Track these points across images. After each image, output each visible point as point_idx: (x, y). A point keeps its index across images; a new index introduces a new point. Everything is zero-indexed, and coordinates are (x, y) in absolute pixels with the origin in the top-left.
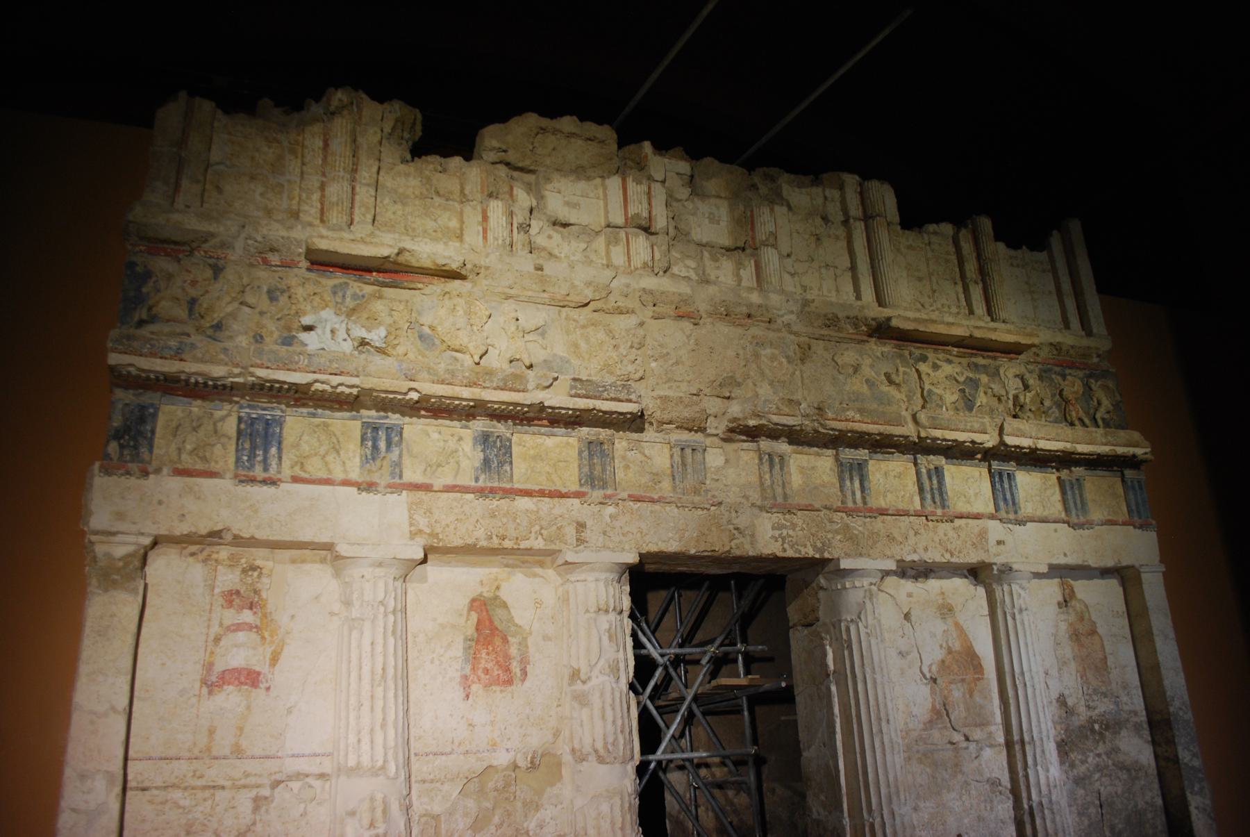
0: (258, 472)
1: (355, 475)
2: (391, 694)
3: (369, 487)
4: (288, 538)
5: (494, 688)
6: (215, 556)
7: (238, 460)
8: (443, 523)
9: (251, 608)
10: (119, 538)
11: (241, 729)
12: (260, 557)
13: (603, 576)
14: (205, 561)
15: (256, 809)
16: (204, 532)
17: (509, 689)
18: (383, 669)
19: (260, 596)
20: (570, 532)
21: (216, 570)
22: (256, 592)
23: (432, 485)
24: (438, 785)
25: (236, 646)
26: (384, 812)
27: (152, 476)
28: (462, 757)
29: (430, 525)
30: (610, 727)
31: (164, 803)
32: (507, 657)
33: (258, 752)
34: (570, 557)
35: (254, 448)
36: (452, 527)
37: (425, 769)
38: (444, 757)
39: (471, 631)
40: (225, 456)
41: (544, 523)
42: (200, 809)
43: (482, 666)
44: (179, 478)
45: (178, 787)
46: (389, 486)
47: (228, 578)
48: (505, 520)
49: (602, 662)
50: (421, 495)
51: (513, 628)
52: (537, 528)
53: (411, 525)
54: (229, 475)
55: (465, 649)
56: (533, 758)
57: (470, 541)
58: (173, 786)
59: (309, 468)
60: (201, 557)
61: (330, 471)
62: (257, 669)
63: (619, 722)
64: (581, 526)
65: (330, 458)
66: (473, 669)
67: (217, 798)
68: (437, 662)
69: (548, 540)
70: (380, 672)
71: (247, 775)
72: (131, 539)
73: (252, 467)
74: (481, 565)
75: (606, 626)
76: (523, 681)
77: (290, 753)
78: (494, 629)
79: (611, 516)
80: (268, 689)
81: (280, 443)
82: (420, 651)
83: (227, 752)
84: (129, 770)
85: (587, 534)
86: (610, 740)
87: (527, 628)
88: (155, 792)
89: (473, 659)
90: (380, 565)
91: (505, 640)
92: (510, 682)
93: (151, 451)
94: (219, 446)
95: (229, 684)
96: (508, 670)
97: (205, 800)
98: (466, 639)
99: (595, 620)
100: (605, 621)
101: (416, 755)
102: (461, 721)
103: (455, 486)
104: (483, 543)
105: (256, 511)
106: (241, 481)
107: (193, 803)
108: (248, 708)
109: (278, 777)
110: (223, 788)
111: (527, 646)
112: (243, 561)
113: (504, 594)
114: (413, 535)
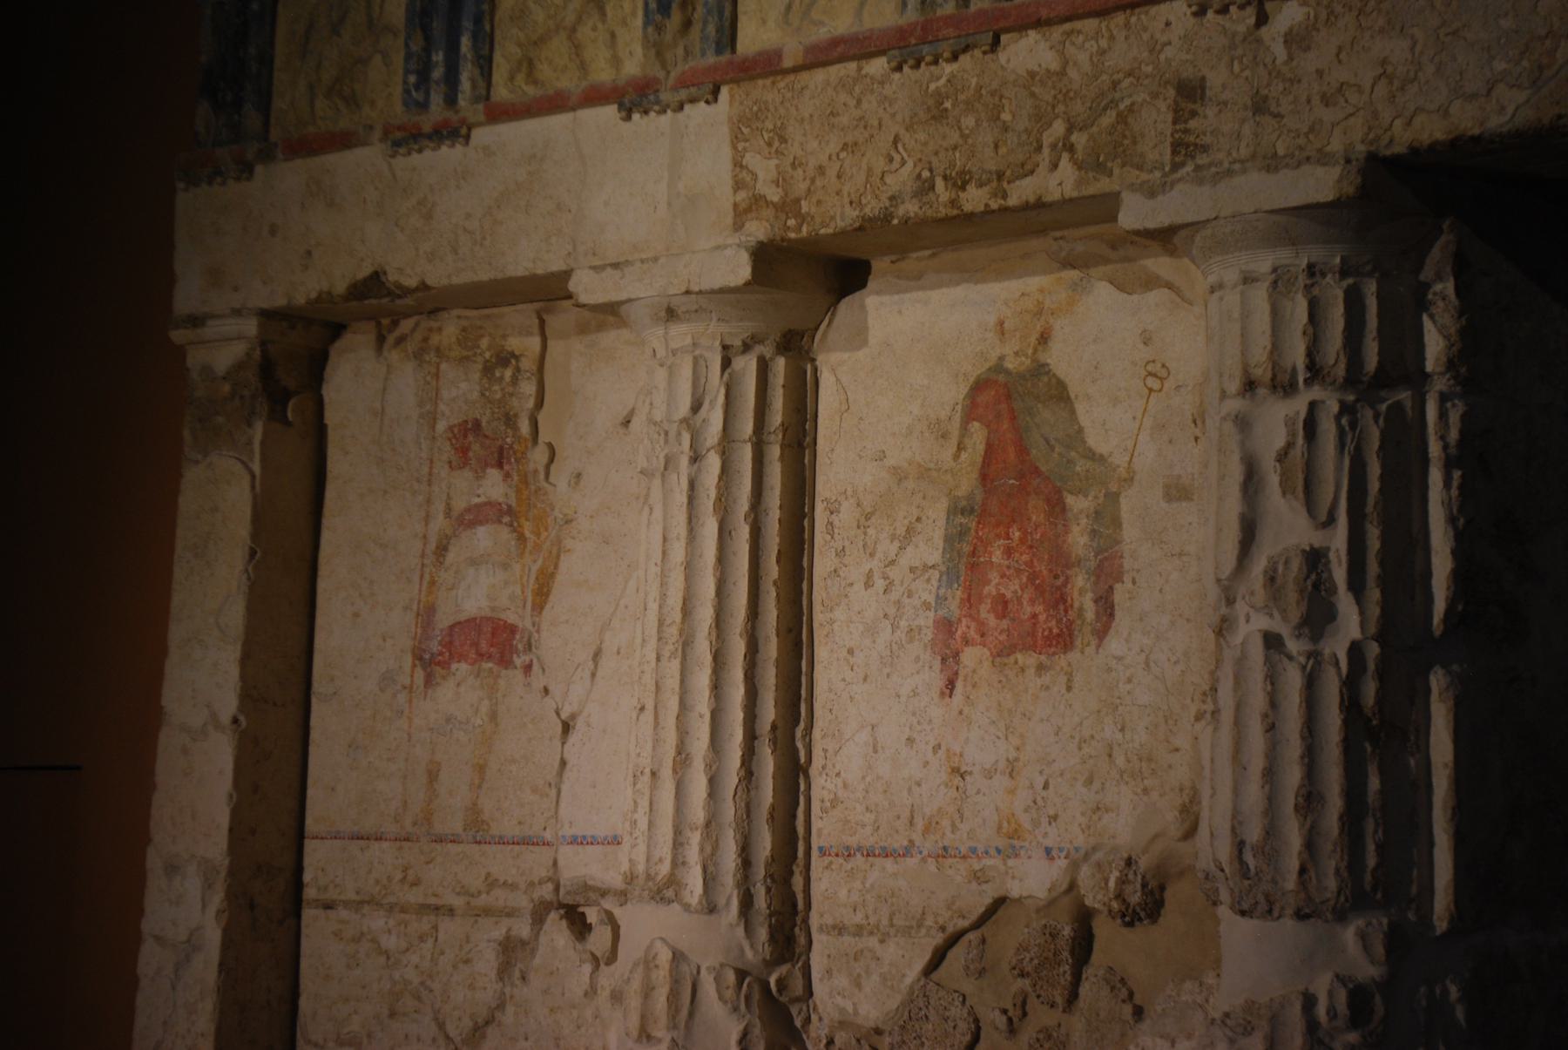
0: (437, 110)
1: (634, 64)
2: (702, 679)
3: (635, 98)
4: (484, 276)
5: (1019, 656)
6: (435, 340)
7: (405, 82)
8: (813, 163)
9: (500, 465)
10: (209, 331)
11: (481, 769)
12: (516, 331)
13: (1263, 263)
14: (418, 355)
15: (504, 971)
16: (340, 287)
17: (1062, 661)
18: (687, 610)
19: (516, 429)
20: (1155, 121)
21: (437, 376)
22: (510, 420)
23: (777, 54)
24: (873, 942)
25: (474, 562)
26: (673, 996)
27: (259, 169)
28: (932, 865)
29: (781, 181)
30: (1254, 792)
31: (357, 940)
32: (1062, 561)
33: (509, 828)
34: (1134, 214)
35: (427, 50)
36: (832, 172)
37: (843, 893)
38: (889, 864)
39: (967, 484)
40: (386, 85)
41: (1079, 108)
42: (415, 959)
43: (990, 589)
44: (299, 162)
45: (379, 905)
46: (683, 83)
47: (461, 391)
48: (969, 122)
49: (1259, 566)
50: (764, 91)
51: (1081, 466)
52: (1059, 127)
53: (738, 185)
54: (377, 134)
55: (948, 539)
56: (1122, 881)
57: (872, 207)
58: (373, 902)
59: (544, 71)
60: (411, 346)
61: (583, 67)
62: (512, 618)
63: (1293, 776)
64: (1190, 92)
65: (585, 32)
66: (970, 602)
67: (441, 936)
68: (880, 584)
69: (1094, 165)
70: (678, 617)
71: (492, 883)
72: (230, 326)
73: (427, 94)
74: (1001, 272)
75: (1280, 442)
76: (1102, 633)
77: (568, 832)
78: (1028, 472)
79: (1290, 39)
80: (528, 668)
81: (478, 20)
82: (841, 553)
83: (456, 825)
84: (307, 861)
85: (1207, 120)
86: (1254, 834)
87: (1120, 460)
88: (344, 913)
89: (965, 564)
90: (671, 314)
91: (1056, 507)
92: (1063, 640)
93: (265, 108)
94: (378, 59)
95: (462, 657)
96: (1059, 600)
97: (422, 939)
98: (954, 510)
99: (1243, 423)
100: (1277, 421)
101: (823, 852)
102: (950, 762)
103: (835, 42)
104: (910, 208)
105: (429, 217)
106: (397, 144)
107: (404, 945)
108: (493, 716)
109: (546, 891)
110: (451, 911)
111: (1117, 523)
112: (484, 343)
113: (1060, 359)
114: (740, 215)
